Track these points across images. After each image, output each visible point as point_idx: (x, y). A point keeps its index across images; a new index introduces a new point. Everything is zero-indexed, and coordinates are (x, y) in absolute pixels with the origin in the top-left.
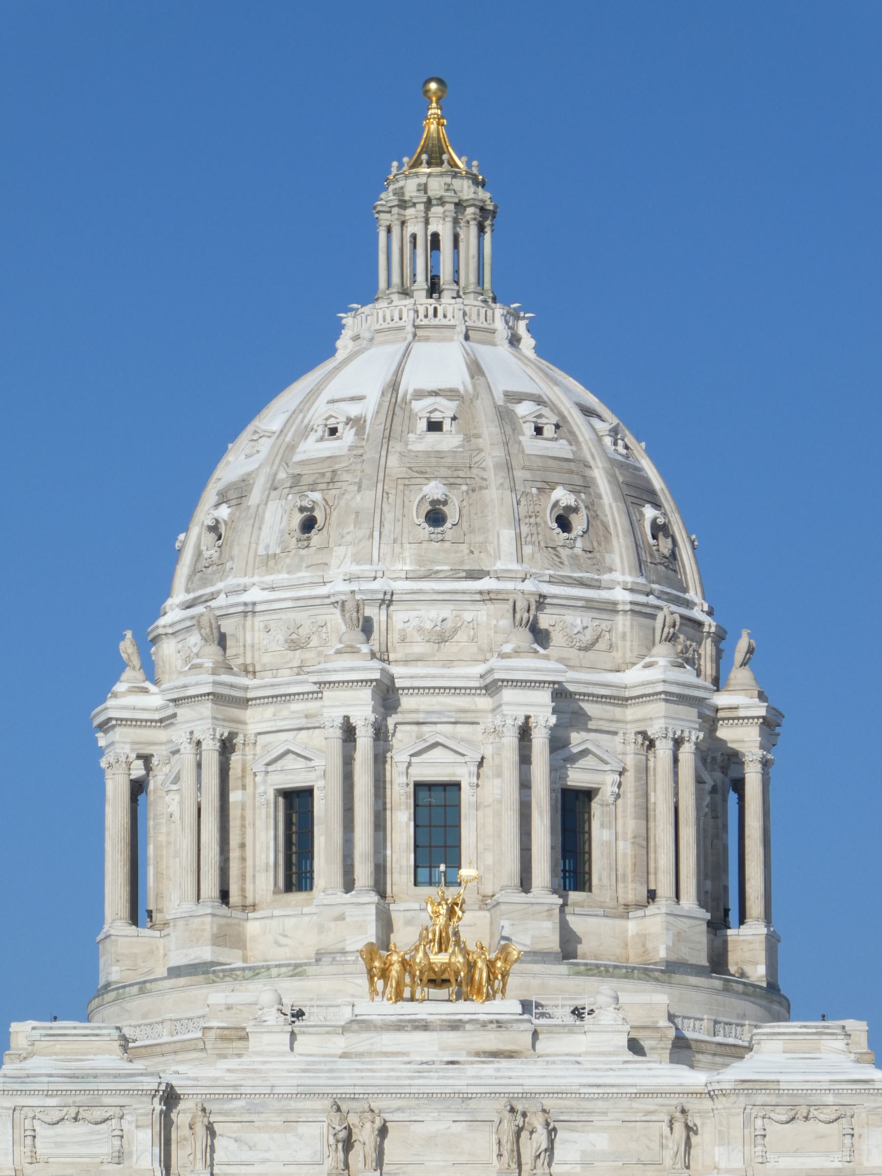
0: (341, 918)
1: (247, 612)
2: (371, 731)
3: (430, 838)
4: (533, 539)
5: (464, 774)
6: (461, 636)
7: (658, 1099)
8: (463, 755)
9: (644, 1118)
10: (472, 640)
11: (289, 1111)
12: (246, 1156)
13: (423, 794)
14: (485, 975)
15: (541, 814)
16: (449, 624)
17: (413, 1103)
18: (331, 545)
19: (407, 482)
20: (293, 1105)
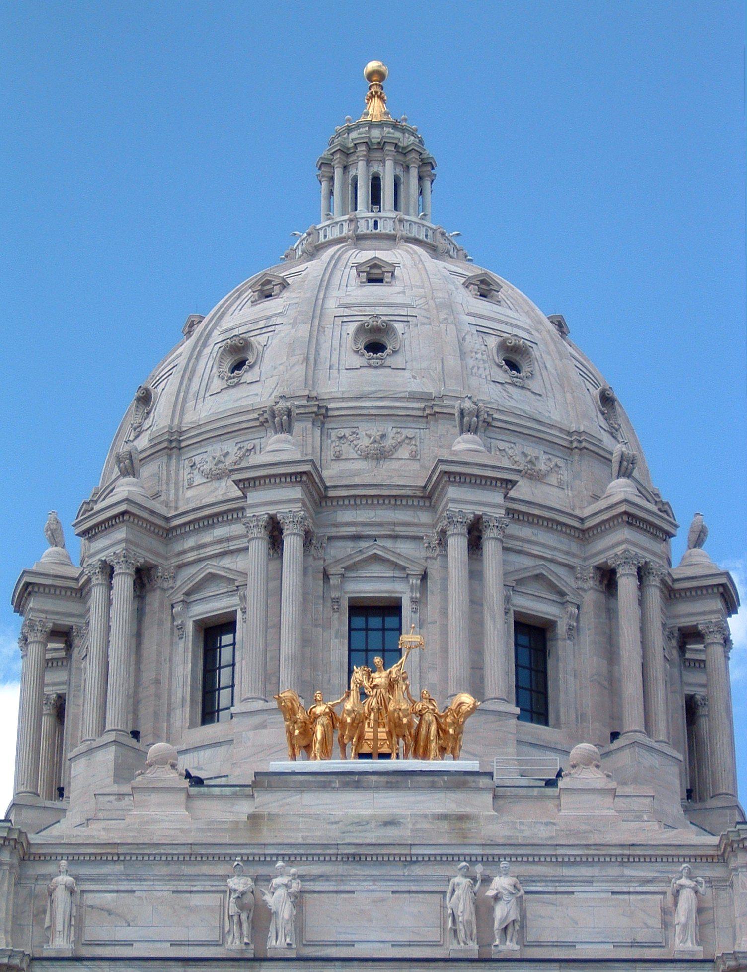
0: (263, 726)
1: (171, 449)
2: (298, 530)
3: (367, 642)
4: (480, 372)
5: (404, 592)
6: (404, 452)
7: (657, 864)
8: (404, 568)
9: (639, 889)
10: (414, 457)
11: (179, 877)
12: (123, 933)
13: (359, 622)
14: (433, 728)
15: (493, 618)
16: (389, 443)
17: (341, 869)
18: (263, 378)
19: (345, 319)
20: (187, 870)
